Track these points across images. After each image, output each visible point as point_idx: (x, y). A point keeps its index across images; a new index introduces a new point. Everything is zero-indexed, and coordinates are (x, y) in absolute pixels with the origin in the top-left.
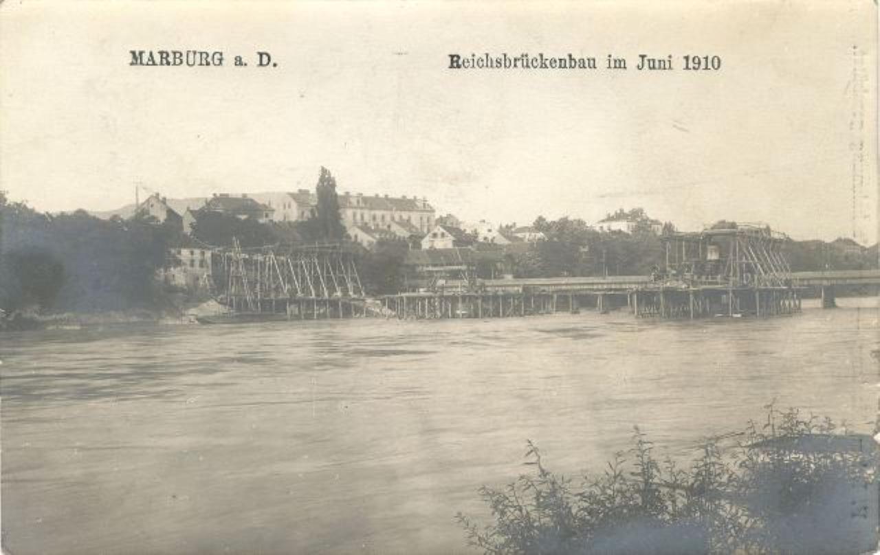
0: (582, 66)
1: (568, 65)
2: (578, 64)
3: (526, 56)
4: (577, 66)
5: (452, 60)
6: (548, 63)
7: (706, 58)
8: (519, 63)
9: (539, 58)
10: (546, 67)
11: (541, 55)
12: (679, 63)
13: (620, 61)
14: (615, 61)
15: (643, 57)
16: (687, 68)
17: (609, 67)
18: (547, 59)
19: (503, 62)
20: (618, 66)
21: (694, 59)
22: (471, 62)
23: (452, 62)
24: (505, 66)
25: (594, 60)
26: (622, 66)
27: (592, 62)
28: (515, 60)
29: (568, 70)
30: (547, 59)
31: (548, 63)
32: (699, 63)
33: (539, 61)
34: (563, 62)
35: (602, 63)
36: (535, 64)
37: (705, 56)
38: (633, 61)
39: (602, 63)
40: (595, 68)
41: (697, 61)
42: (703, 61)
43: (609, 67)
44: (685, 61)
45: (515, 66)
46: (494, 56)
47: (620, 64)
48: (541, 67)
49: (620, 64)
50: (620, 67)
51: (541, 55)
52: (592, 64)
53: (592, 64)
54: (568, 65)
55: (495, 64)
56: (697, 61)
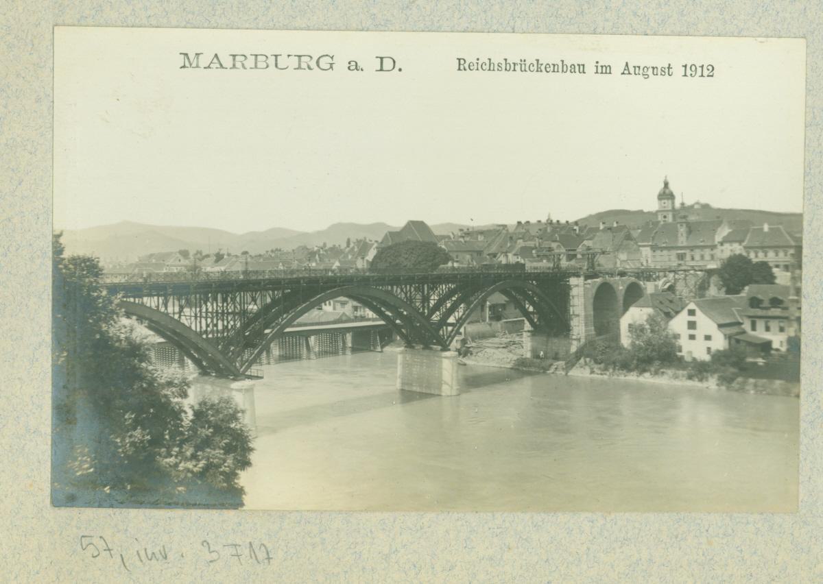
0: (573, 70)
1: (560, 70)
2: (569, 68)
3: (525, 61)
4: (569, 70)
5: (459, 62)
6: (543, 68)
7: (702, 67)
8: (518, 68)
9: (535, 63)
10: (541, 71)
11: (538, 61)
12: (678, 71)
13: (606, 68)
14: (602, 67)
15: (685, 66)
16: (685, 75)
17: (597, 72)
18: (542, 64)
19: (503, 67)
20: (604, 71)
21: (691, 68)
22: (476, 65)
23: (460, 64)
24: (506, 69)
25: (583, 65)
26: (608, 71)
27: (581, 67)
28: (514, 64)
29: (560, 73)
30: (542, 64)
31: (543, 68)
32: (696, 68)
33: (536, 65)
34: (556, 67)
35: (590, 69)
36: (532, 68)
37: (701, 65)
38: (618, 68)
39: (590, 69)
40: (584, 73)
41: (693, 68)
42: (699, 70)
43: (597, 72)
44: (684, 68)
45: (514, 70)
46: (495, 61)
47: (605, 70)
48: (537, 71)
49: (605, 70)
50: (606, 73)
51: (538, 61)
52: (582, 68)
53: (582, 68)
54: (560, 70)
55: (496, 67)
56: (693, 68)
